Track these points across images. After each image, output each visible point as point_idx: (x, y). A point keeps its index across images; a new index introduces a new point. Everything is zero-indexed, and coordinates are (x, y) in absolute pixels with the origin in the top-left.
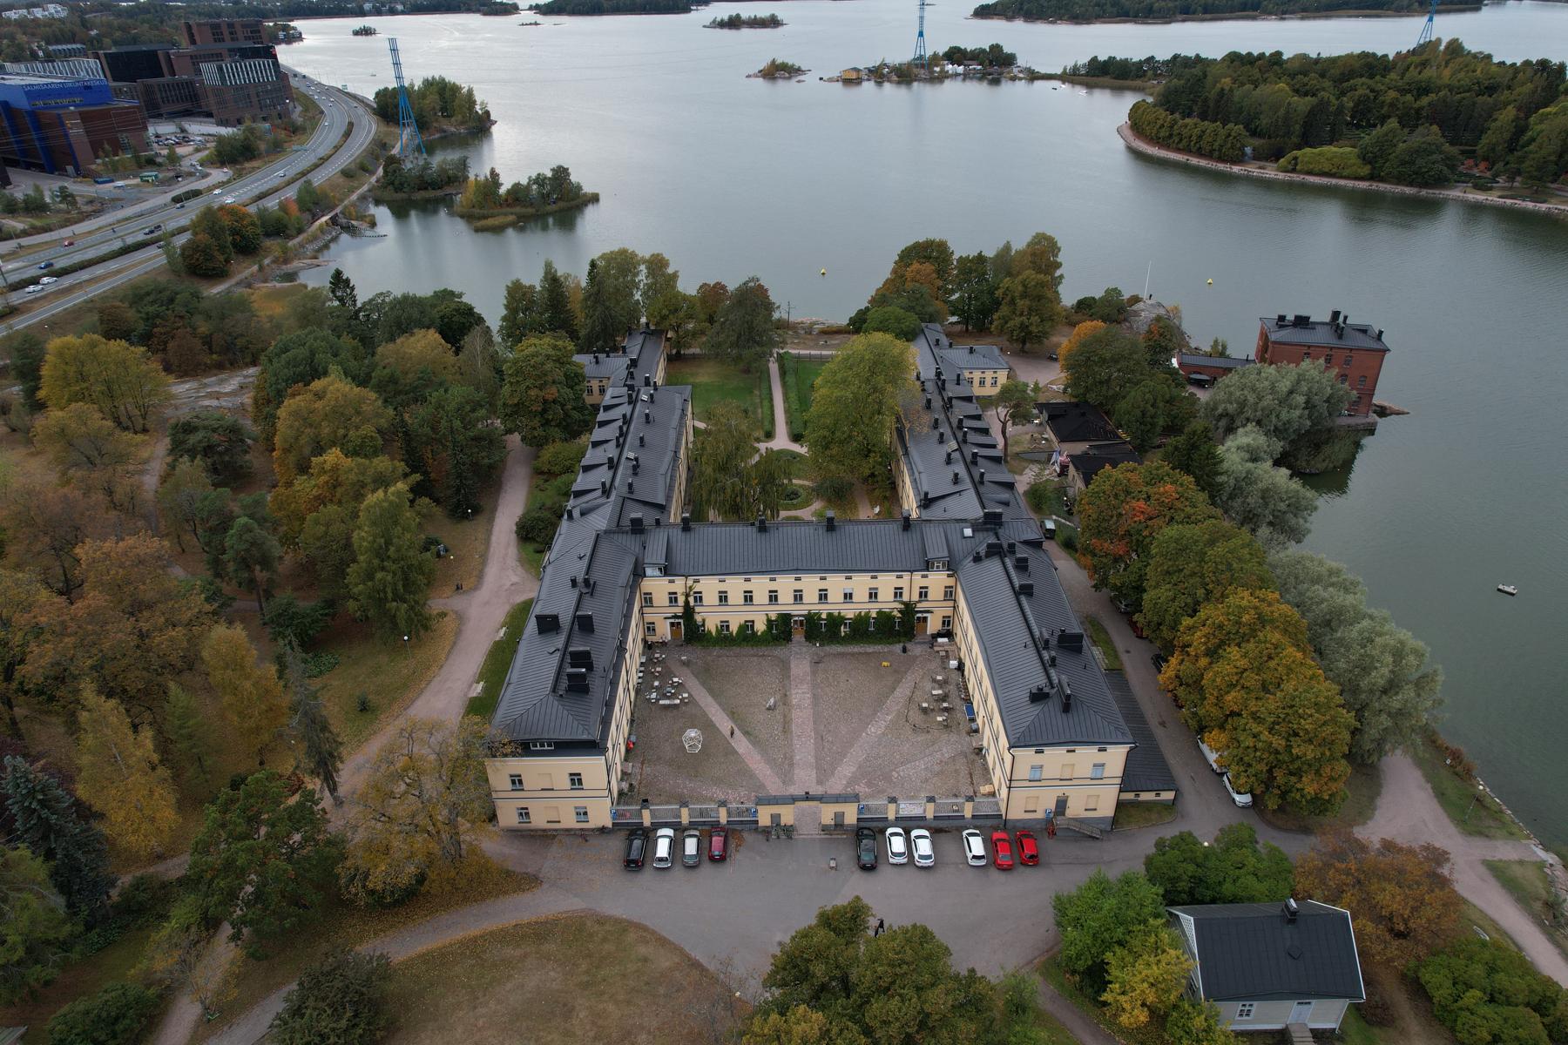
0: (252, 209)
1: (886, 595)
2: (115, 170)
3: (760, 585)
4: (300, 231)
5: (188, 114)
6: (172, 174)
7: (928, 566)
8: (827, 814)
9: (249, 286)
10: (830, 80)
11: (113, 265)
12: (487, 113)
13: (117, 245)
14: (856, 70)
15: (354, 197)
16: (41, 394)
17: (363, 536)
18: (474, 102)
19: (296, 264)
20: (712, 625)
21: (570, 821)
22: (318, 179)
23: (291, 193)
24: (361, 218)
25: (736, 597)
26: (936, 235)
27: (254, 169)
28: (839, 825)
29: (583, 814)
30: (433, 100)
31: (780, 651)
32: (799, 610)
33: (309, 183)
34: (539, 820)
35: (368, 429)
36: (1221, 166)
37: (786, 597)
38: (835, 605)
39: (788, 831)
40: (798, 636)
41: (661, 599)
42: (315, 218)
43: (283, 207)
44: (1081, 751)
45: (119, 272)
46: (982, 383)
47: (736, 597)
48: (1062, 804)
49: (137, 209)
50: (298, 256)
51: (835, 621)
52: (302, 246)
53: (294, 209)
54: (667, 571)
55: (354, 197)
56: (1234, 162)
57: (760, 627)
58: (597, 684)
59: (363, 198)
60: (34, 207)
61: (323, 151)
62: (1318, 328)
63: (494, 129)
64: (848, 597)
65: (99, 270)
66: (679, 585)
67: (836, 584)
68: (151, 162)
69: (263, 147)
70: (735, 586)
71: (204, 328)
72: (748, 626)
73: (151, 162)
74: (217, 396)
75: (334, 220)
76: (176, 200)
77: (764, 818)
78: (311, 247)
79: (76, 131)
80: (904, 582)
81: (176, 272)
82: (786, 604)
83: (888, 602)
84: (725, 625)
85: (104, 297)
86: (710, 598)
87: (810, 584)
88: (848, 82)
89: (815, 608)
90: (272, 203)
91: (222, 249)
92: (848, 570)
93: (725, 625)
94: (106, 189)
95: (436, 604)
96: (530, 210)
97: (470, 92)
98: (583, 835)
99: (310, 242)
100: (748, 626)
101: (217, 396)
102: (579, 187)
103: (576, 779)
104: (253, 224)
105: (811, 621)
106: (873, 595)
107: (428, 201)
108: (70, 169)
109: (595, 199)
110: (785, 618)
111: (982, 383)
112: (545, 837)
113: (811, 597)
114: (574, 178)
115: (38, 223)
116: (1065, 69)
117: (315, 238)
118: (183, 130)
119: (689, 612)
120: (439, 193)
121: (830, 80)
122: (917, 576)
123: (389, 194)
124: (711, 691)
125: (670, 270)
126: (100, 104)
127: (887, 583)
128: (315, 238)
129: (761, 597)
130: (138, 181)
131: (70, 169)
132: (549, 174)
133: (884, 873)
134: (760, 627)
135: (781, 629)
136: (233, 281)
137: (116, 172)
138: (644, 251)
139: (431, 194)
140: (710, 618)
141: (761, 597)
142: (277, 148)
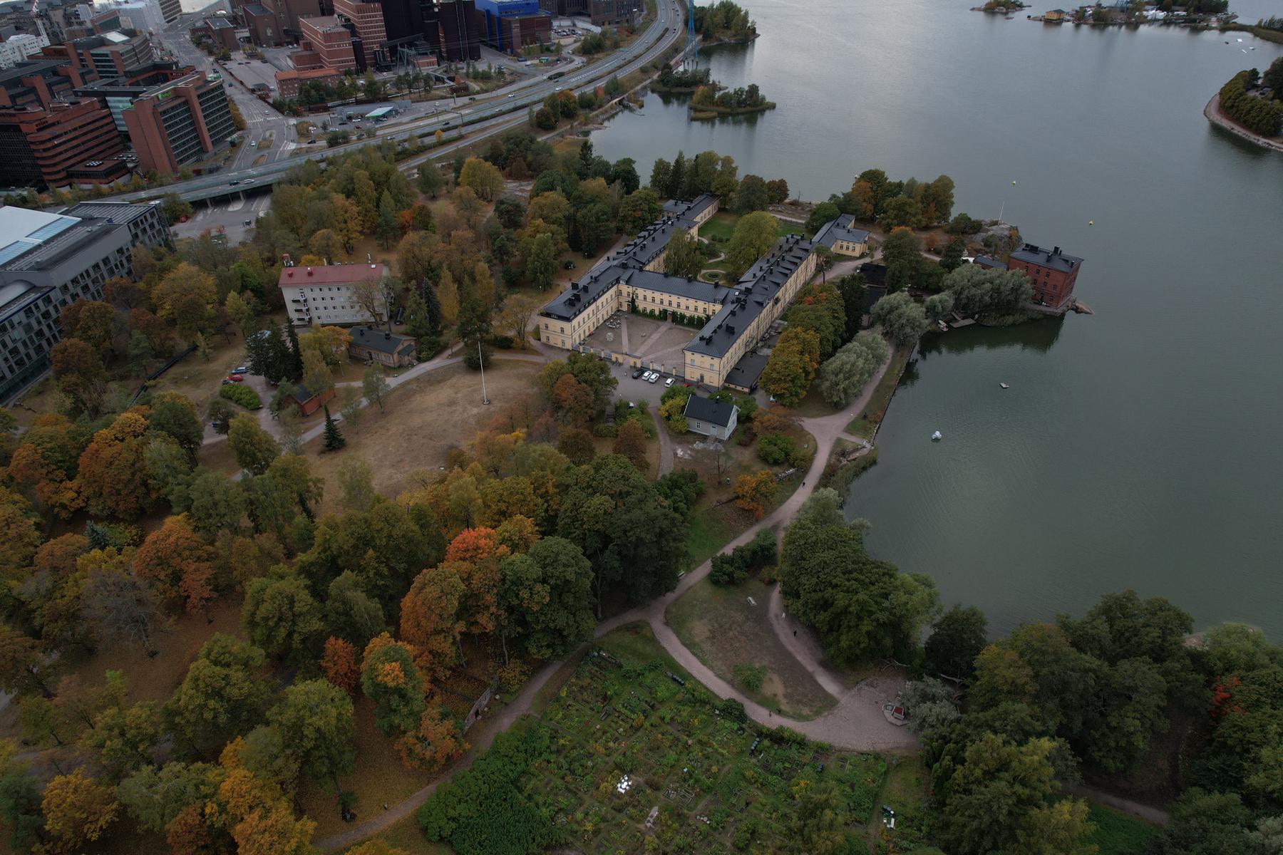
0: (576, 94)
1: (700, 310)
2: (529, 54)
3: (658, 295)
4: (600, 107)
5: (580, 14)
6: (556, 58)
7: (715, 302)
8: (631, 361)
9: (562, 137)
10: (1035, 19)
11: (507, 117)
12: (754, 30)
13: (512, 106)
14: (1059, 12)
15: (638, 88)
16: (459, 180)
17: (534, 248)
18: (747, 22)
19: (590, 127)
20: (641, 308)
21: (560, 345)
22: (621, 75)
23: (602, 84)
24: (635, 102)
25: (649, 299)
26: (882, 169)
27: (598, 59)
28: (635, 367)
29: (563, 342)
30: (720, 18)
31: (660, 323)
32: (670, 309)
33: (616, 78)
34: (552, 342)
35: (559, 215)
36: (1252, 137)
37: (666, 303)
38: (681, 310)
39: (620, 364)
40: (669, 320)
41: (625, 294)
42: (612, 99)
43: (596, 93)
44: (706, 357)
45: (508, 121)
46: (848, 248)
47: (649, 299)
48: (702, 377)
49: (532, 81)
50: (592, 122)
51: (683, 316)
52: (597, 116)
53: (601, 94)
54: (628, 282)
55: (638, 88)
56: (1265, 135)
57: (657, 313)
58: (578, 306)
59: (645, 88)
60: (485, 77)
61: (636, 53)
62: (1041, 254)
63: (758, 40)
64: (687, 308)
65: (500, 120)
66: (631, 289)
67: (683, 300)
68: (548, 49)
69: (608, 43)
70: (649, 294)
71: (530, 158)
72: (652, 311)
73: (548, 49)
74: (522, 191)
75: (620, 102)
76: (550, 78)
77: (614, 359)
78: (601, 117)
79: (516, 30)
80: (706, 306)
81: (532, 125)
82: (666, 306)
83: (700, 313)
84: (645, 309)
85: (498, 135)
86: (641, 297)
87: (675, 299)
88: (1049, 22)
89: (676, 310)
90: (589, 90)
91: (555, 115)
92: (688, 296)
93: (645, 309)
94: (520, 66)
95: (556, 282)
96: (729, 110)
97: (747, 13)
98: (562, 350)
99: (602, 114)
100: (652, 311)
101: (522, 191)
102: (763, 98)
103: (562, 330)
104: (575, 102)
105: (674, 313)
106: (696, 309)
107: (681, 94)
108: (509, 50)
109: (773, 106)
110: (665, 311)
111: (848, 248)
112: (552, 347)
113: (674, 304)
114: (760, 93)
115: (484, 88)
116: (1260, 22)
117: (606, 112)
118: (574, 25)
119: (633, 301)
120: (688, 90)
121: (1035, 19)
122: (711, 304)
123: (660, 87)
124: (628, 328)
125: (734, 165)
126: (530, 14)
127: (701, 305)
128: (606, 112)
129: (658, 301)
130: (536, 62)
131: (509, 50)
132: (747, 88)
133: (639, 381)
134: (657, 313)
135: (664, 315)
136: (556, 133)
137: (530, 55)
138: (722, 154)
139: (683, 90)
140: (641, 305)
141: (658, 301)
142: (616, 46)
